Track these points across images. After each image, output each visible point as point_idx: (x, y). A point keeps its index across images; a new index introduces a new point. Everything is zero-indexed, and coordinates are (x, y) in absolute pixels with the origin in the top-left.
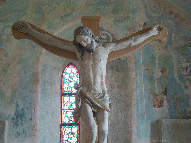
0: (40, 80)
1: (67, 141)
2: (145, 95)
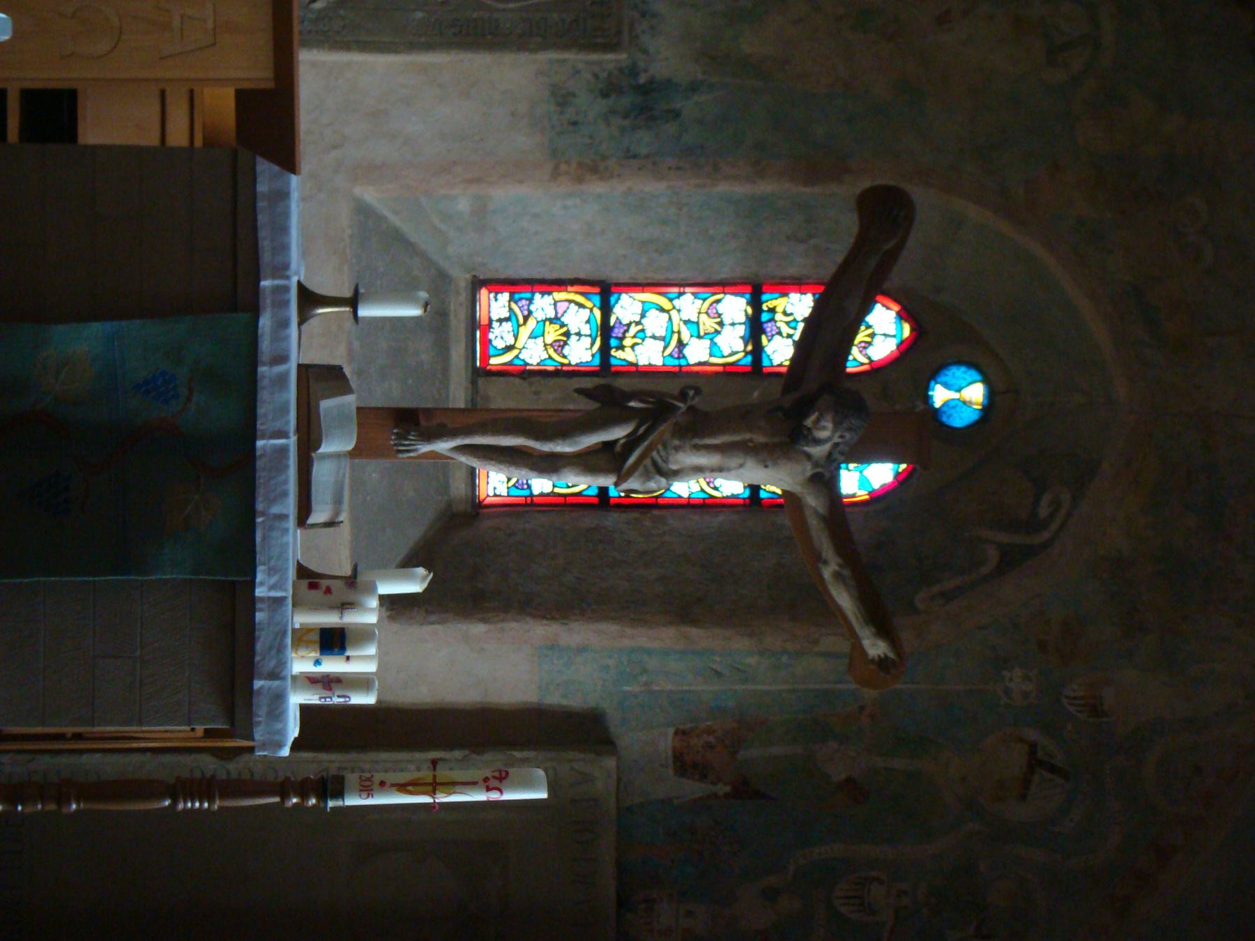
0: (817, 189)
1: (526, 313)
2: (735, 691)
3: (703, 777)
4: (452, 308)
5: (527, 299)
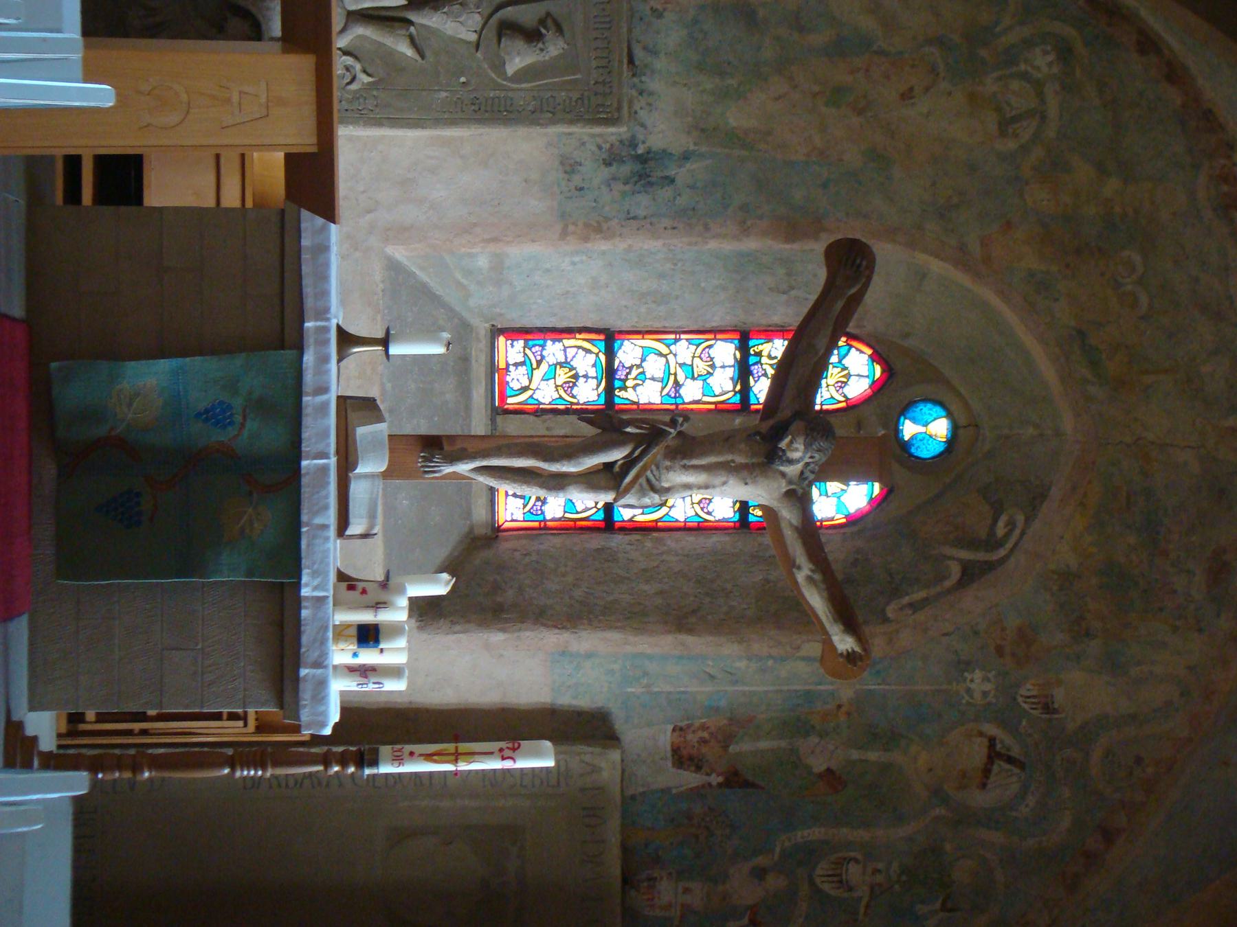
0: (796, 246)
2: (726, 691)
3: (698, 768)
4: (473, 353)
5: (540, 346)
